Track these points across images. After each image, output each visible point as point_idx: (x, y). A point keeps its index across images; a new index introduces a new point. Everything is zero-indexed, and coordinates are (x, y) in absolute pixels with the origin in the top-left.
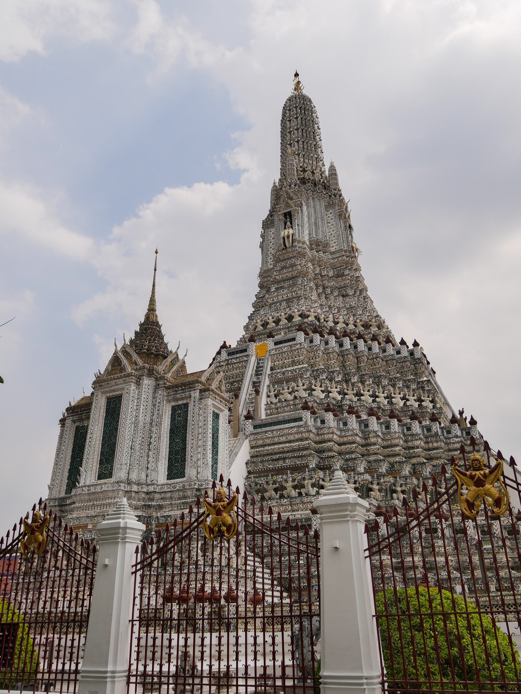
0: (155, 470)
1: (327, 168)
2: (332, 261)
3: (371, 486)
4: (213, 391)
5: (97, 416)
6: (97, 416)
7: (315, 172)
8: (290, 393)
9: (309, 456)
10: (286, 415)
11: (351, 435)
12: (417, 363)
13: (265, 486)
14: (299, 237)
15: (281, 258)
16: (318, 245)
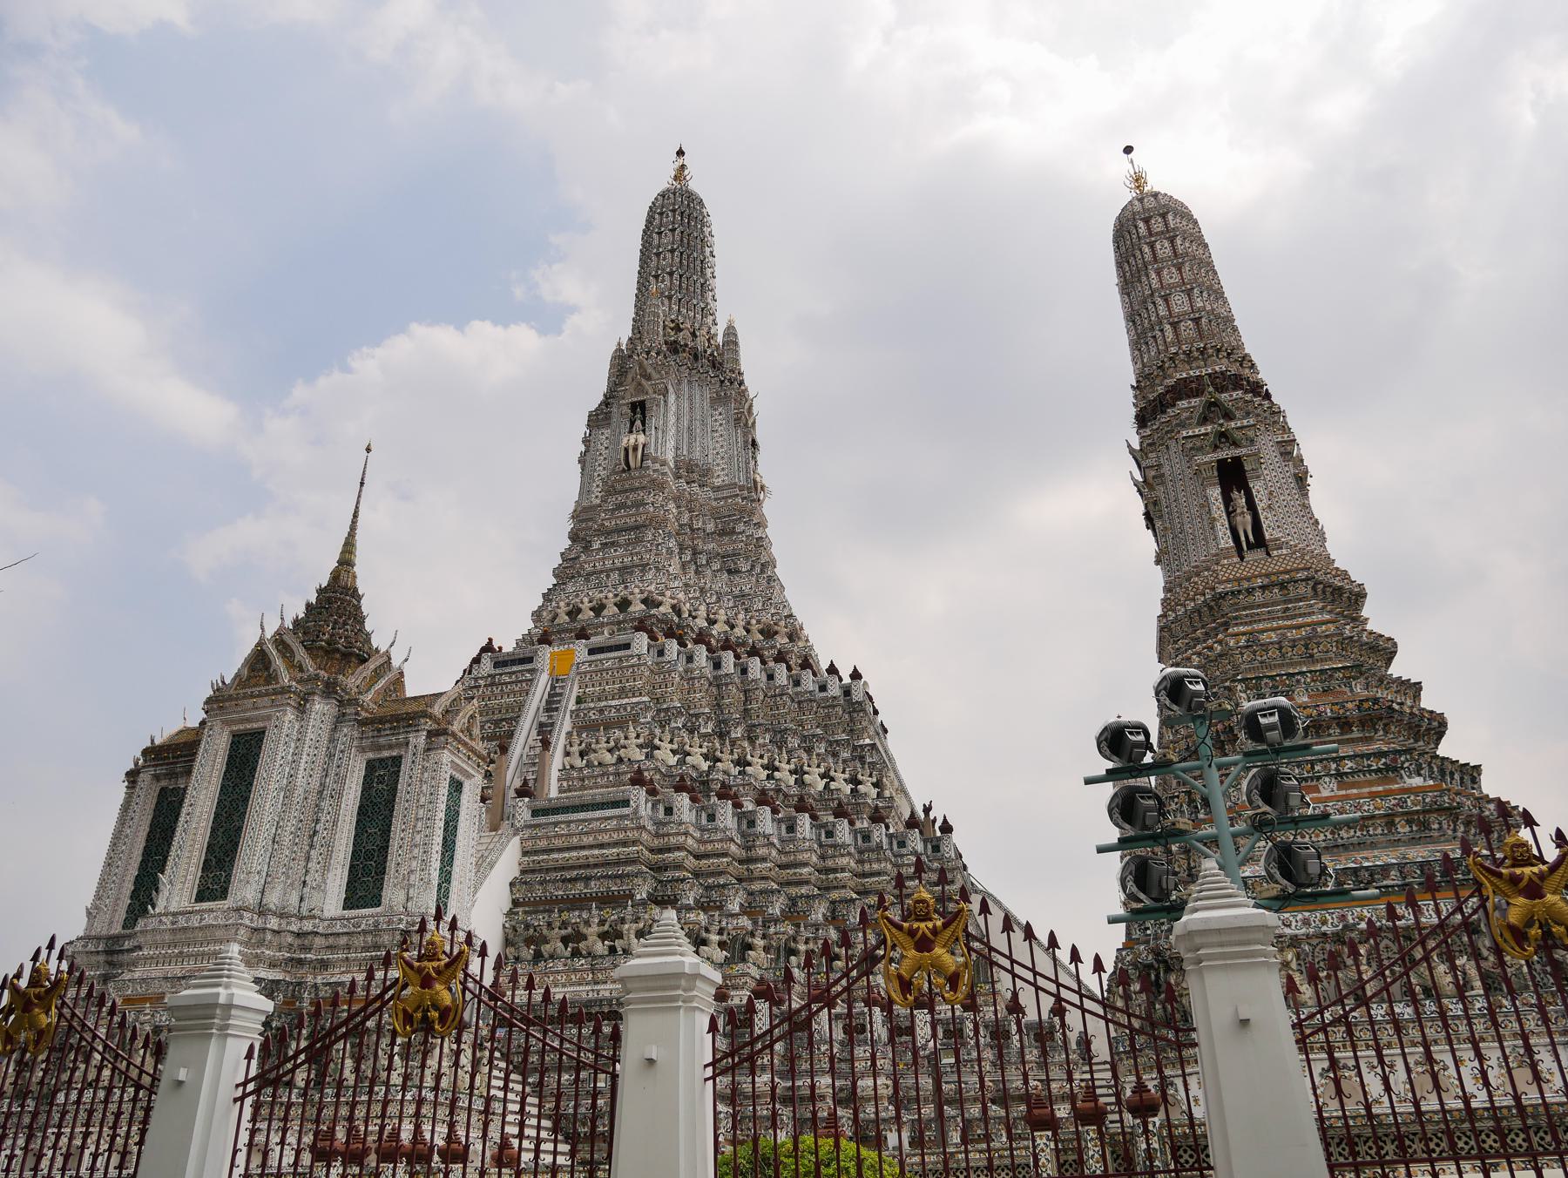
0: (321, 888)
1: (720, 330)
2: (714, 504)
4: (454, 735)
5: (208, 769)
6: (208, 769)
8: (609, 751)
10: (598, 794)
11: (721, 840)
13: (545, 932)
15: (618, 487)
16: (690, 470)
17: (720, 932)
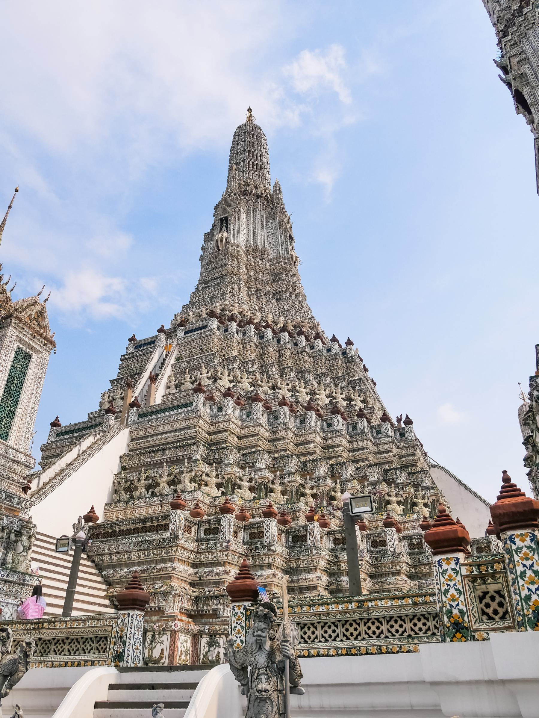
1: (271, 189)
3: (271, 486)
7: (258, 187)
9: (192, 445)
11: (254, 426)
12: (349, 362)
13: (136, 483)
14: (234, 240)
17: (250, 480)
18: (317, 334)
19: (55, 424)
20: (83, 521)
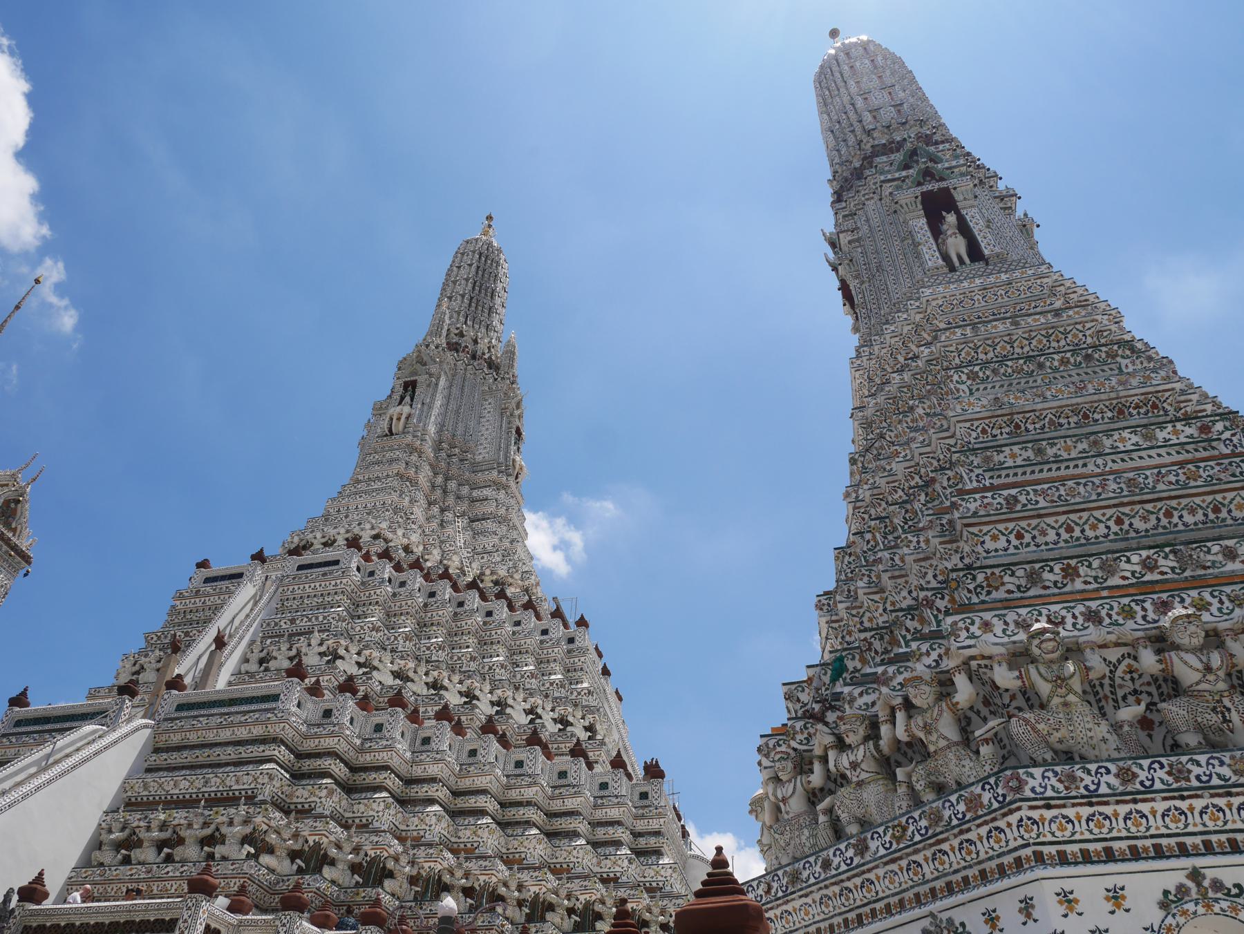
18: (530, 601)
19: (19, 700)
20: (15, 898)
